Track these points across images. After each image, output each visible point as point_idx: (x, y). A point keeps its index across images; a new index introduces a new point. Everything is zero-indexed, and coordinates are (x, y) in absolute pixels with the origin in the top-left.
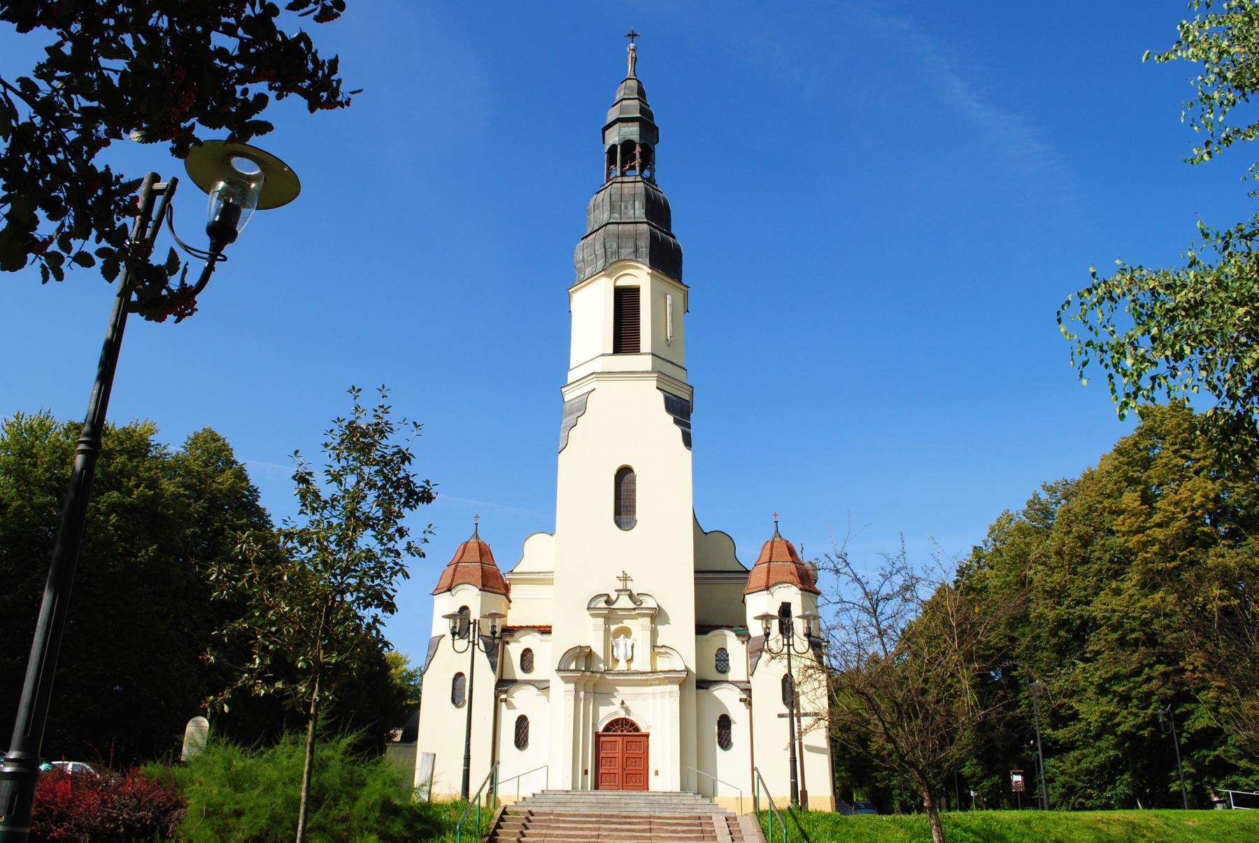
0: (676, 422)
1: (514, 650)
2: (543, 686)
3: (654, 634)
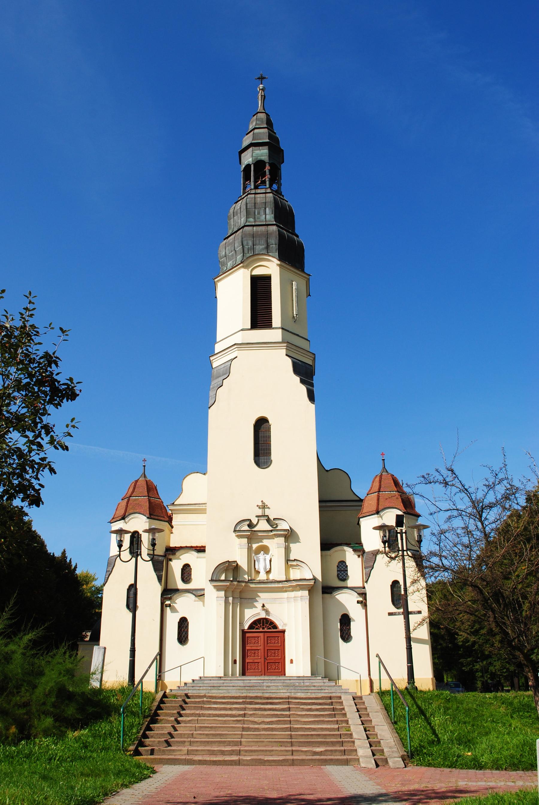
0: (302, 381)
1: (176, 566)
2: (199, 594)
3: (287, 550)
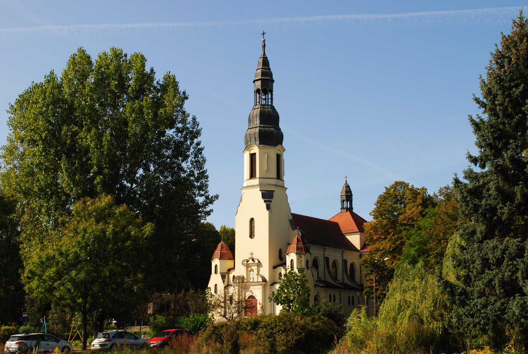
3: (258, 271)
